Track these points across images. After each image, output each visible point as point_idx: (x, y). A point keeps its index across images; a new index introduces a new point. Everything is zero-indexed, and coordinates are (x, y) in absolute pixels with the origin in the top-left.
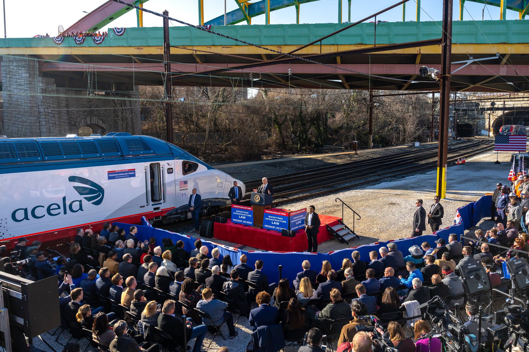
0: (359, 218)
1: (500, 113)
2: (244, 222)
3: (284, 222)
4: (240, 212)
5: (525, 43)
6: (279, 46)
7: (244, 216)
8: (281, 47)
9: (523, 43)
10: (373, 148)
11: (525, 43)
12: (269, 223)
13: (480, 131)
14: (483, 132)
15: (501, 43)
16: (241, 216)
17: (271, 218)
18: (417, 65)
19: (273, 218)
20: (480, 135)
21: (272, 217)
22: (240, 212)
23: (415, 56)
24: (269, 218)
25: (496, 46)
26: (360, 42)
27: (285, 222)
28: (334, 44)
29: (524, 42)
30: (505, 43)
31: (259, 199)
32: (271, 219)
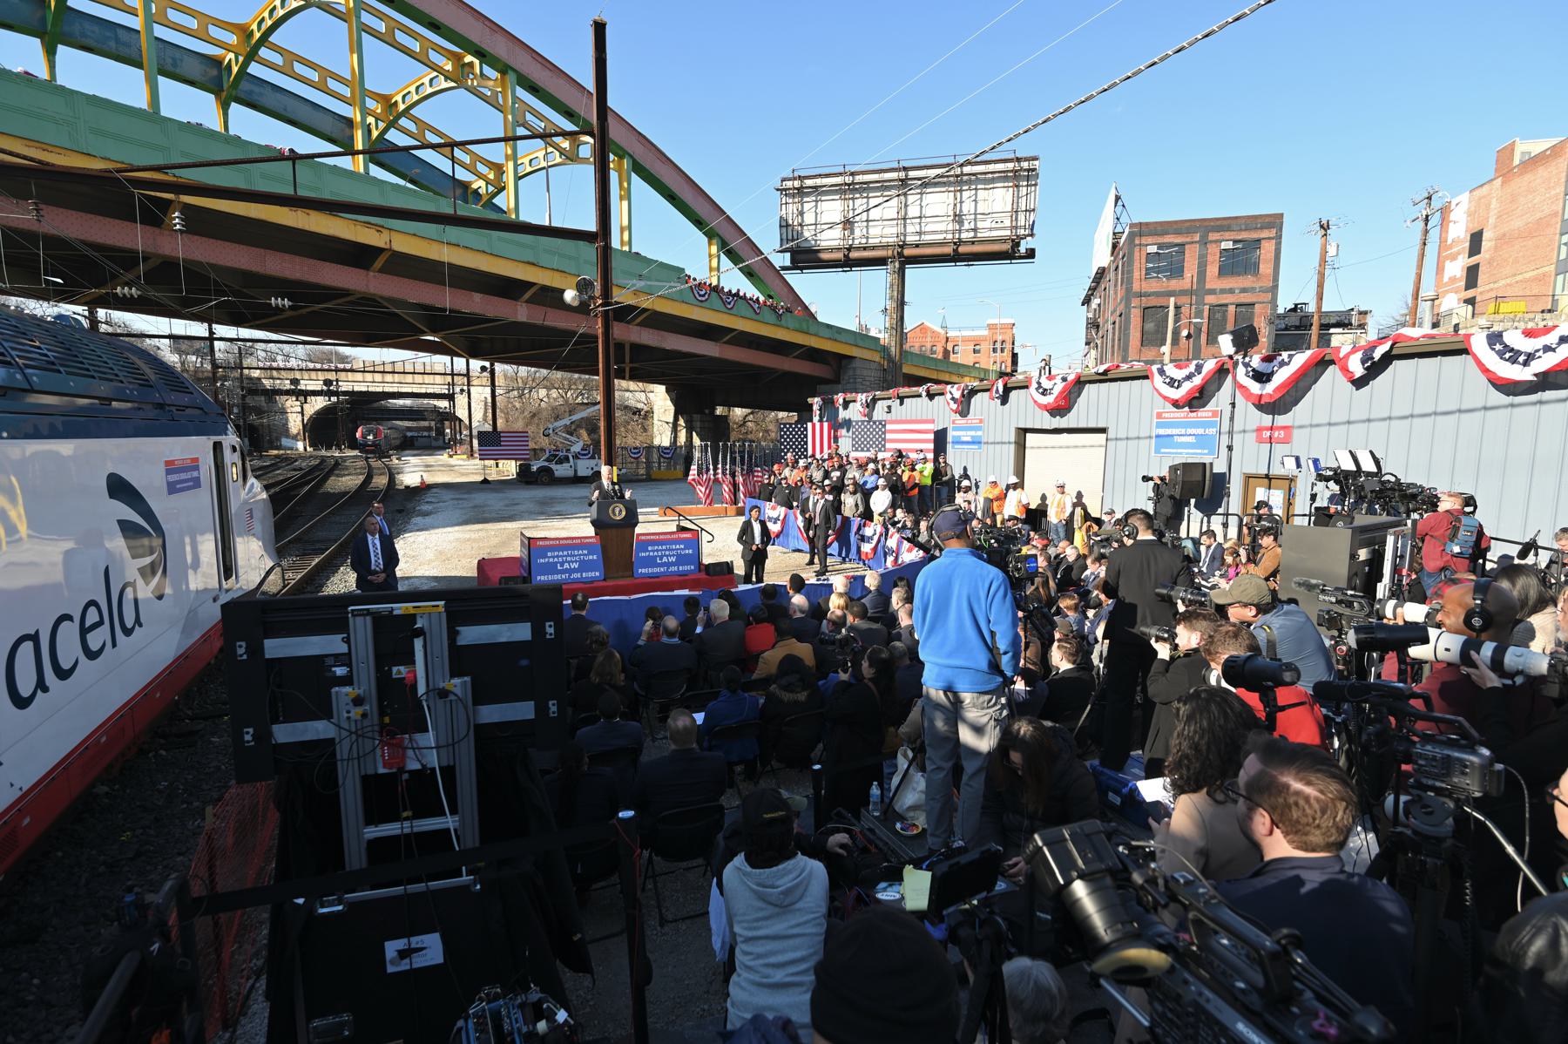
0: (710, 538)
1: (319, 403)
2: (576, 575)
3: (687, 552)
4: (561, 553)
7: (573, 562)
12: (651, 562)
13: (278, 439)
14: (285, 442)
15: (528, 263)
16: (562, 564)
17: (653, 551)
18: (372, 274)
20: (278, 448)
22: (561, 553)
23: (374, 252)
25: (521, 265)
27: (691, 551)
31: (624, 513)
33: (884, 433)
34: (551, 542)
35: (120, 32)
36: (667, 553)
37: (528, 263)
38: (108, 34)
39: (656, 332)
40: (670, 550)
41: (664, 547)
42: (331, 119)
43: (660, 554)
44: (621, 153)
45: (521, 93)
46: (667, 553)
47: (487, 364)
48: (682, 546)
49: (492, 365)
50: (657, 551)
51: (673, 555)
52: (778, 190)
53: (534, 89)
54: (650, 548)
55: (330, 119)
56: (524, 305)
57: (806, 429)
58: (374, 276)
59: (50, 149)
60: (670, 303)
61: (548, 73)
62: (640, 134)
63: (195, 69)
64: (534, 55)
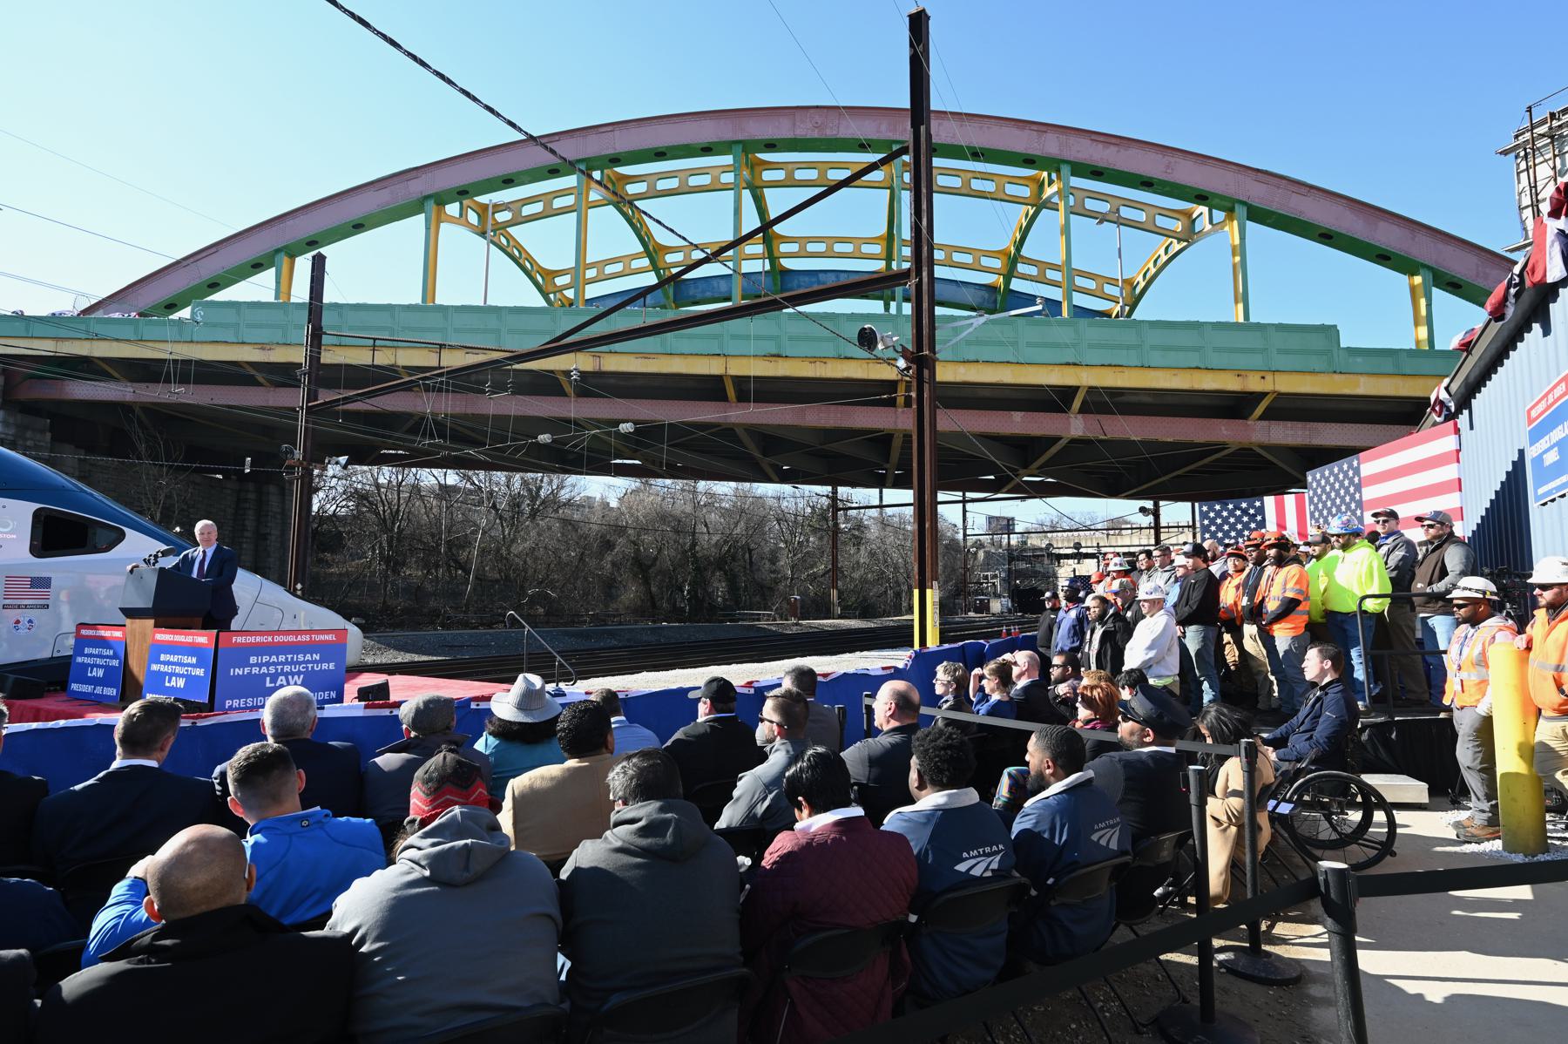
5: (1115, 366)
6: (597, 354)
8: (599, 357)
9: (1110, 365)
10: (840, 617)
11: (1115, 366)
15: (1068, 364)
17: (260, 665)
19: (274, 664)
21: (265, 659)
24: (256, 665)
25: (1057, 368)
26: (774, 352)
28: (719, 355)
29: (1113, 364)
30: (1075, 364)
32: (264, 670)
33: (1358, 488)
34: (259, 639)
35: (821, 275)
36: (287, 668)
37: (1068, 364)
38: (813, 280)
39: (1299, 425)
40: (292, 663)
41: (282, 658)
42: (973, 290)
43: (272, 670)
44: (1229, 205)
45: (1076, 182)
46: (287, 668)
47: (1149, 504)
48: (317, 657)
49: (1156, 505)
50: (268, 664)
51: (299, 673)
52: (1505, 153)
53: (1097, 174)
54: (253, 660)
55: (972, 290)
56: (1080, 416)
57: (1261, 511)
58: (903, 412)
59: (648, 356)
60: (1308, 378)
61: (1113, 149)
62: (1258, 170)
63: (969, 296)
64: (1093, 137)
